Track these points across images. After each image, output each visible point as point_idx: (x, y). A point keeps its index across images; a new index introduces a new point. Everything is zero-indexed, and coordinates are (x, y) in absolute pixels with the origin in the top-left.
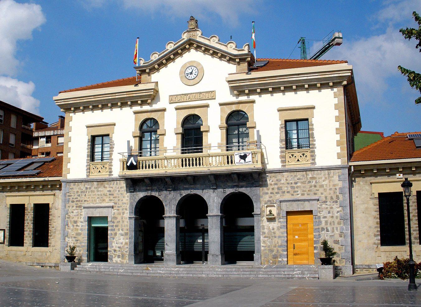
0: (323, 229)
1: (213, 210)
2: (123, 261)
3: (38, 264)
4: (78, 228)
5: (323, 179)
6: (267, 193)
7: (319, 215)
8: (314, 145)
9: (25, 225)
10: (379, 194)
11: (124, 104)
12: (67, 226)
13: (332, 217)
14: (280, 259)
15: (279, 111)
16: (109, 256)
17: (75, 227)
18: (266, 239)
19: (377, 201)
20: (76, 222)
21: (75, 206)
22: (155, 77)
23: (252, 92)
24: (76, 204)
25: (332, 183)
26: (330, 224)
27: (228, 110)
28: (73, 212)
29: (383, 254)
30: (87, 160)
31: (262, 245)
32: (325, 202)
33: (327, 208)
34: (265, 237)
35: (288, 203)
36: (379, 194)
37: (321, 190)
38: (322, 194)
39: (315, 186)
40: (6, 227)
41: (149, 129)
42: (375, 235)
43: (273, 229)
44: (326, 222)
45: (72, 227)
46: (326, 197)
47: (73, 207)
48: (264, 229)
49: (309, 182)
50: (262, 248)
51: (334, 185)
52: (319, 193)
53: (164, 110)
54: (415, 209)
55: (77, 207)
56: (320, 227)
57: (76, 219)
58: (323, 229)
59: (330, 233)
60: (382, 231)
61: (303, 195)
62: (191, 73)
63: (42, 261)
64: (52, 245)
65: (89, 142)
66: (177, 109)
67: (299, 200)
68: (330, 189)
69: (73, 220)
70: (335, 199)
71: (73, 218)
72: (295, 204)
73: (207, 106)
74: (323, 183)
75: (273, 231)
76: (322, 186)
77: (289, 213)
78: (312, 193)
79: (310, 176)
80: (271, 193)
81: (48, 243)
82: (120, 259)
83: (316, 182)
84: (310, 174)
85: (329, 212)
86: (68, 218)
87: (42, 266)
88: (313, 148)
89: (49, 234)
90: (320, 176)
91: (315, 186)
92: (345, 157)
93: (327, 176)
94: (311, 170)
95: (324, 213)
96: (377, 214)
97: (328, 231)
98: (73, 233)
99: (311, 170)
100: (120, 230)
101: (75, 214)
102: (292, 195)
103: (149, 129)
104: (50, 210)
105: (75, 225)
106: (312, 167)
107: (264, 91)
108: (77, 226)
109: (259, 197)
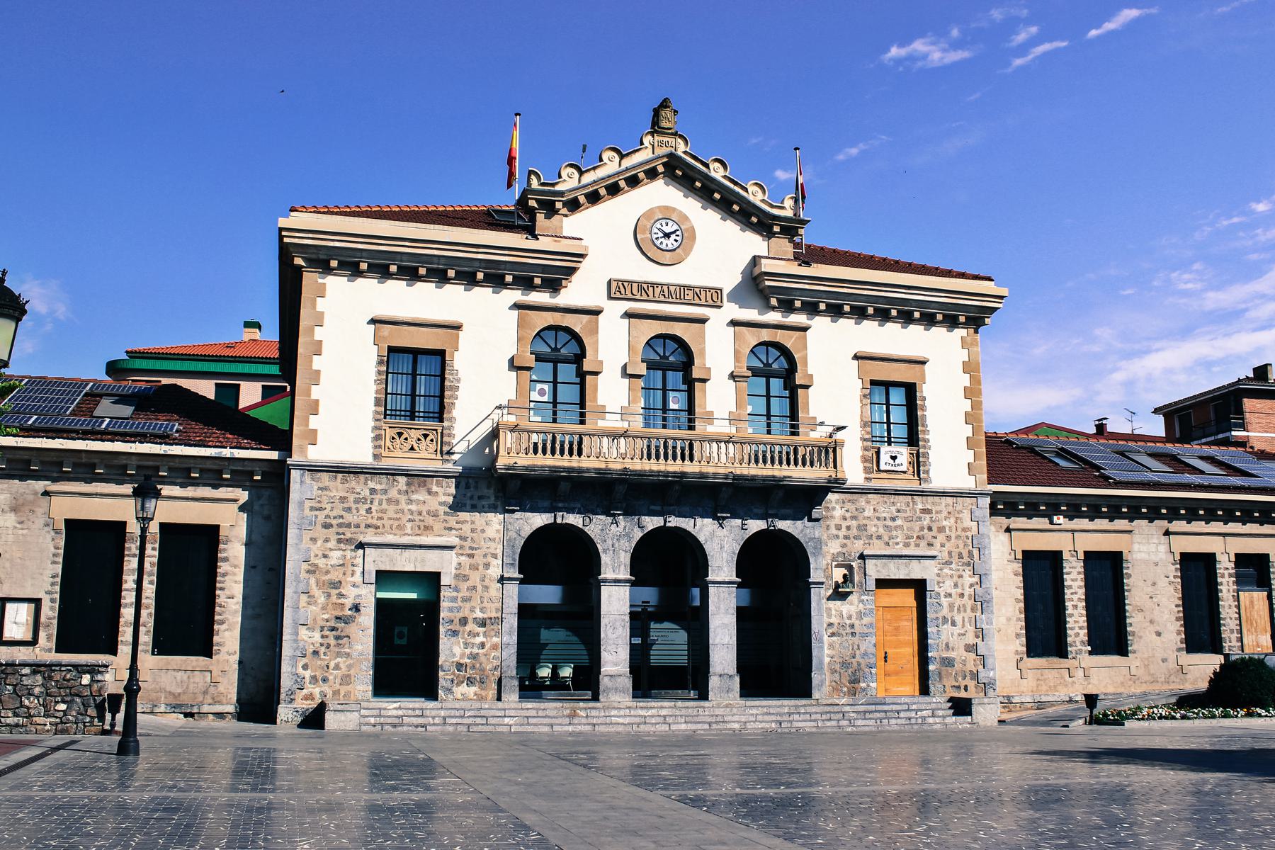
0: (945, 620)
1: (720, 568)
2: (483, 693)
3: (175, 708)
4: (342, 601)
5: (945, 514)
6: (837, 537)
7: (937, 589)
8: (927, 441)
9: (125, 586)
10: (1086, 553)
11: (496, 280)
12: (304, 598)
13: (962, 595)
14: (863, 685)
15: (856, 357)
16: (442, 682)
17: (334, 599)
18: (834, 638)
19: (1018, 567)
20: (337, 585)
21: (334, 538)
22: (571, 224)
23: (811, 309)
24: (338, 534)
25: (960, 526)
26: (959, 610)
27: (752, 338)
28: (325, 556)
29: (1030, 675)
30: (377, 412)
31: (826, 652)
32: (948, 563)
33: (951, 576)
34: (833, 634)
35: (879, 562)
36: (1086, 553)
37: (941, 537)
38: (943, 545)
39: (930, 529)
40: (48, 593)
41: (560, 354)
42: (1018, 636)
43: (850, 617)
44: (951, 606)
45: (322, 600)
46: (950, 553)
47: (327, 540)
48: (829, 616)
49: (920, 519)
50: (827, 660)
51: (964, 530)
52: (937, 543)
53: (596, 312)
54: (1080, 587)
55: (339, 541)
56: (940, 615)
57: (335, 576)
58: (945, 620)
59: (957, 630)
60: (1028, 628)
61: (907, 545)
62: (667, 235)
63: (185, 699)
64: (224, 650)
65: (380, 363)
66: (629, 315)
67: (900, 557)
68: (958, 537)
69: (327, 578)
70: (966, 559)
71: (327, 572)
72: (892, 564)
73: (703, 321)
74: (945, 523)
75: (848, 622)
76: (942, 529)
77: (882, 584)
78: (923, 543)
79: (920, 506)
80: (846, 537)
81: (211, 645)
82: (473, 689)
83: (932, 521)
84: (920, 503)
85: (956, 586)
86: (308, 572)
87: (188, 715)
88: (924, 447)
89: (217, 618)
90: (938, 508)
91: (930, 529)
92: (982, 473)
93: (950, 509)
94: (922, 494)
95: (948, 586)
96: (1020, 594)
97: (953, 624)
98: (326, 616)
99: (922, 494)
100: (478, 611)
101: (334, 561)
102: (887, 544)
103: (560, 354)
104: (221, 546)
105: (334, 592)
106: (925, 486)
107: (836, 312)
108: (341, 595)
109: (819, 543)
